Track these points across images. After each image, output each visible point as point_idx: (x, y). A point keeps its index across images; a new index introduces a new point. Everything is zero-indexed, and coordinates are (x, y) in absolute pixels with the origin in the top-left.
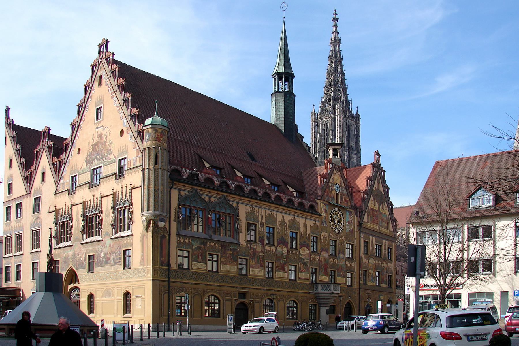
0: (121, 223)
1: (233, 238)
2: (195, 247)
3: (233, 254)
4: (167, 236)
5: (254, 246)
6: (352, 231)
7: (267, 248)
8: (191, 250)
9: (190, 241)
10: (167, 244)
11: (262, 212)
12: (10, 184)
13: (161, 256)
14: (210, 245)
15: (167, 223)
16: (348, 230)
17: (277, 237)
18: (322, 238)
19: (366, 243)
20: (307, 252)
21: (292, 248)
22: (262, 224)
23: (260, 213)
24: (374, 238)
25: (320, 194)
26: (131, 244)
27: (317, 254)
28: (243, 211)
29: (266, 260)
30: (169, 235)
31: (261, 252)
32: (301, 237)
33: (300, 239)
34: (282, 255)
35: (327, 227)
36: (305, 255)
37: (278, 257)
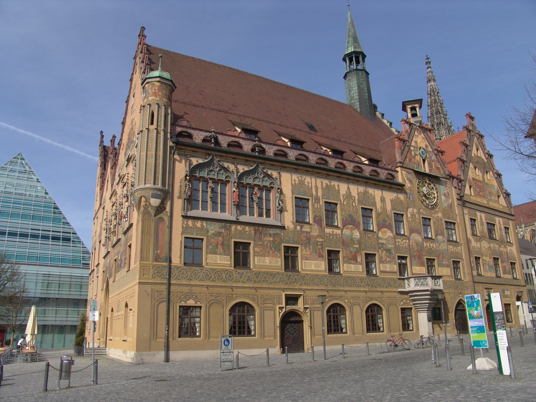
2: (211, 232)
3: (274, 241)
4: (166, 219)
5: (306, 228)
6: (451, 206)
7: (328, 230)
9: (204, 224)
10: (167, 231)
11: (316, 184)
13: (156, 247)
14: (236, 229)
16: (446, 205)
17: (342, 215)
18: (409, 215)
19: (473, 220)
20: (389, 234)
21: (366, 230)
22: (317, 199)
23: (314, 184)
24: (483, 215)
25: (398, 159)
27: (405, 237)
29: (327, 248)
31: (319, 236)
32: (378, 215)
33: (377, 218)
34: (352, 239)
35: (414, 201)
36: (386, 239)
37: (346, 243)
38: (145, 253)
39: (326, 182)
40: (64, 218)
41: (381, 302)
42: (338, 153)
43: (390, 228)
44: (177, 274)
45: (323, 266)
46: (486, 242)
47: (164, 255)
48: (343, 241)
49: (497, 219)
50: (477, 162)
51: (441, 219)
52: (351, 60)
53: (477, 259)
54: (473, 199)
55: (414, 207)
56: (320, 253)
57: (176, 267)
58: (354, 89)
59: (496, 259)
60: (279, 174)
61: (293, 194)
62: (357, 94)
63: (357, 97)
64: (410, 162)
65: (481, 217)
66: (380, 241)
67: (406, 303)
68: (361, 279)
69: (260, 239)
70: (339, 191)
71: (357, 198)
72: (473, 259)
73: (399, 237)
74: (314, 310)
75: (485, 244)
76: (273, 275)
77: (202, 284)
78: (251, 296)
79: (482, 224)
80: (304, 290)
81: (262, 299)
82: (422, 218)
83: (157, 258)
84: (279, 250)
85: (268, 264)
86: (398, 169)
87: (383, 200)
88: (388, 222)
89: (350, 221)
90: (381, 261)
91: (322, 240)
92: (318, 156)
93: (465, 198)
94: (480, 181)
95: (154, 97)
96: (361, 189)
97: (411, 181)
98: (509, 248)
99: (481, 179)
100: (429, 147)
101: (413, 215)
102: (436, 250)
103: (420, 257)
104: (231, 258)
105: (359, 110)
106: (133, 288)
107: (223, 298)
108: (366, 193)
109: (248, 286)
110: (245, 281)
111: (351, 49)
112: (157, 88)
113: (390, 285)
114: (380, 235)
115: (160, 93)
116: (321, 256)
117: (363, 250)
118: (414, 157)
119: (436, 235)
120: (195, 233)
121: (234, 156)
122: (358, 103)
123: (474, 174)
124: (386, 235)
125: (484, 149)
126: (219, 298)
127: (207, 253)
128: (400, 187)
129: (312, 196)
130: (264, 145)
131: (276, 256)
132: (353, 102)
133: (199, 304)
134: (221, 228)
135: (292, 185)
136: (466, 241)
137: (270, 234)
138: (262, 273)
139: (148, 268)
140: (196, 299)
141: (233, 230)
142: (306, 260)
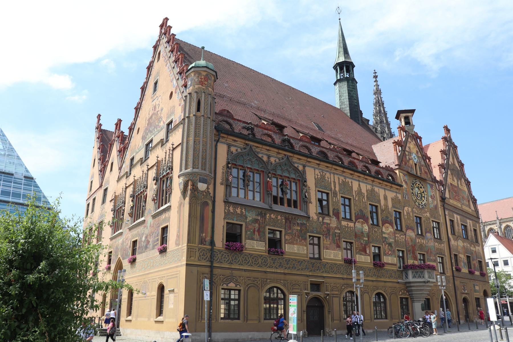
0: (163, 196)
1: (300, 209)
2: (249, 219)
3: (301, 231)
4: (210, 203)
5: (327, 220)
6: (436, 207)
7: (344, 223)
8: (244, 224)
9: (243, 211)
10: (210, 214)
11: (335, 179)
12: (92, 182)
13: (202, 230)
14: (270, 216)
15: (211, 187)
16: (432, 206)
17: (355, 210)
18: (405, 213)
19: (452, 221)
20: (391, 229)
22: (335, 194)
24: (459, 217)
26: (168, 219)
27: (402, 233)
28: (311, 176)
29: (343, 240)
30: (214, 202)
31: (336, 228)
32: (382, 211)
33: (381, 214)
34: (362, 233)
36: (388, 234)
37: (358, 235)
38: (192, 235)
39: (342, 178)
40: (44, 197)
41: (385, 292)
42: (349, 153)
43: (391, 224)
44: (220, 257)
45: (340, 256)
46: (461, 241)
47: (208, 239)
48: (356, 234)
49: (468, 221)
50: (453, 170)
51: (429, 218)
52: (341, 69)
53: (456, 256)
54: (452, 202)
55: (409, 206)
56: (337, 244)
57: (219, 250)
58: (345, 95)
59: (468, 257)
60: (304, 167)
61: (316, 187)
62: (348, 100)
63: (348, 103)
64: (405, 165)
65: (457, 218)
66: (384, 235)
67: (404, 293)
68: (370, 269)
69: (290, 228)
70: (352, 187)
71: (366, 195)
72: (453, 256)
73: (398, 232)
74: (333, 297)
75: (460, 243)
76: (300, 262)
77: (241, 268)
78: (282, 281)
79: (458, 225)
80: (324, 277)
81: (292, 284)
82: (415, 216)
83: (202, 241)
84: (305, 239)
85: (296, 252)
86: (397, 172)
87: (386, 198)
88: (390, 218)
89: (361, 216)
90: (385, 254)
91: (339, 232)
92: (335, 154)
93: (446, 201)
94: (455, 187)
95: (200, 86)
96: (369, 187)
97: (406, 183)
98: (477, 248)
99: (456, 185)
100: (419, 153)
101: (408, 213)
102: (425, 246)
103: (414, 253)
104: (266, 244)
105: (349, 115)
106: (179, 269)
107: (259, 283)
108: (373, 190)
109: (279, 271)
110: (277, 266)
111: (342, 59)
112: (203, 77)
113: (391, 276)
114: (384, 230)
115: (206, 83)
116: (338, 246)
117: (371, 243)
118: (409, 161)
119: (426, 233)
120: (235, 219)
121: (268, 148)
122: (348, 108)
123: (451, 180)
124: (388, 230)
125: (458, 158)
126: (255, 282)
127: (246, 239)
128: (399, 187)
129: (331, 190)
130: (292, 141)
131: (303, 245)
132: (343, 106)
133: (238, 287)
134: (258, 215)
135: (315, 179)
136: (447, 240)
137: (298, 223)
138: (291, 260)
139: (194, 250)
140: (237, 283)
141: (267, 217)
142: (327, 249)
